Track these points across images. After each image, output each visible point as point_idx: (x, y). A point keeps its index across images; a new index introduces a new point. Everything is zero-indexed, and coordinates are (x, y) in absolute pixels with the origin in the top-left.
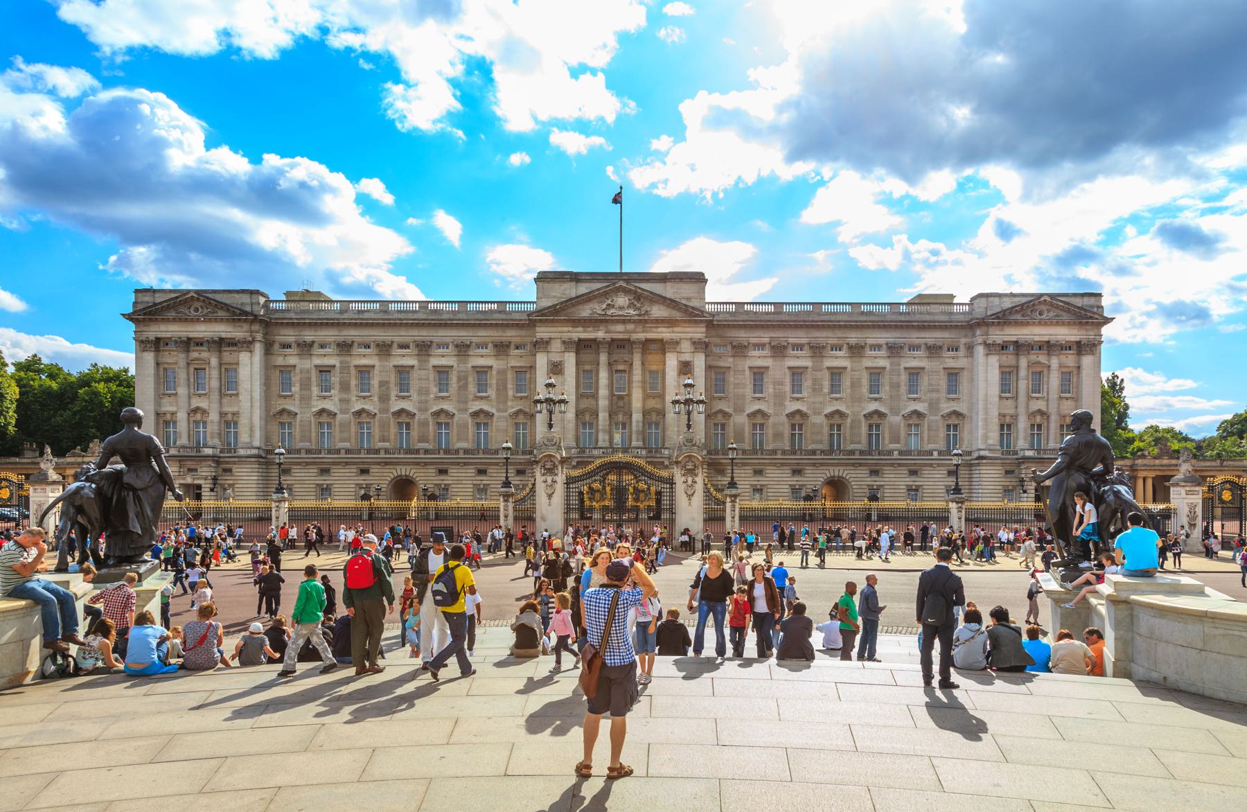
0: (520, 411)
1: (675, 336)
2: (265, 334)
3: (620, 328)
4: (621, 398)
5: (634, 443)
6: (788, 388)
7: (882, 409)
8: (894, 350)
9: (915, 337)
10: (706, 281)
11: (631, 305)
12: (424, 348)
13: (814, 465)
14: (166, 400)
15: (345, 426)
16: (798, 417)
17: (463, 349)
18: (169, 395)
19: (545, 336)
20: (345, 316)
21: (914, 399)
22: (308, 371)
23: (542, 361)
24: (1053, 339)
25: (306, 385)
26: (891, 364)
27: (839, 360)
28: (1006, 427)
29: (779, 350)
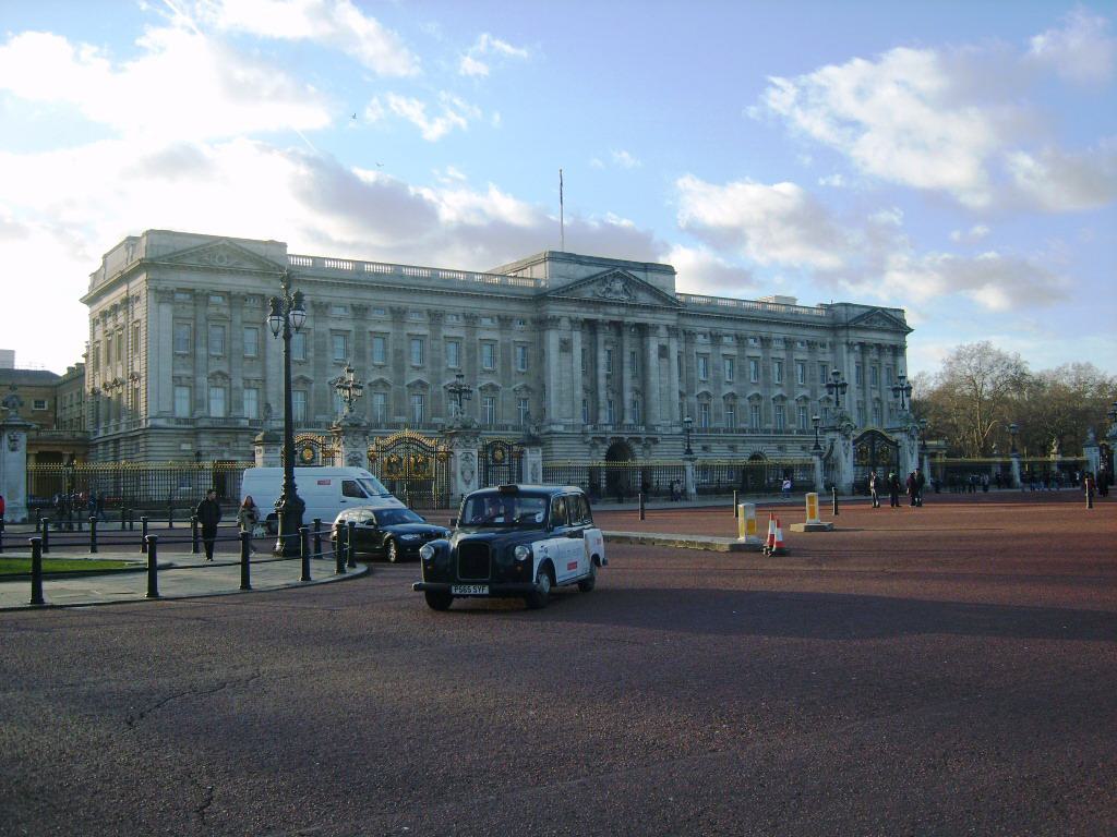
0: (525, 386)
3: (615, 310)
8: (789, 343)
10: (674, 273)
12: (436, 317)
13: (744, 442)
17: (471, 320)
18: (184, 356)
19: (557, 314)
20: (362, 278)
21: (802, 386)
22: (324, 335)
23: (553, 339)
25: (321, 351)
26: (788, 355)
27: (755, 351)
28: (861, 409)
29: (716, 339)
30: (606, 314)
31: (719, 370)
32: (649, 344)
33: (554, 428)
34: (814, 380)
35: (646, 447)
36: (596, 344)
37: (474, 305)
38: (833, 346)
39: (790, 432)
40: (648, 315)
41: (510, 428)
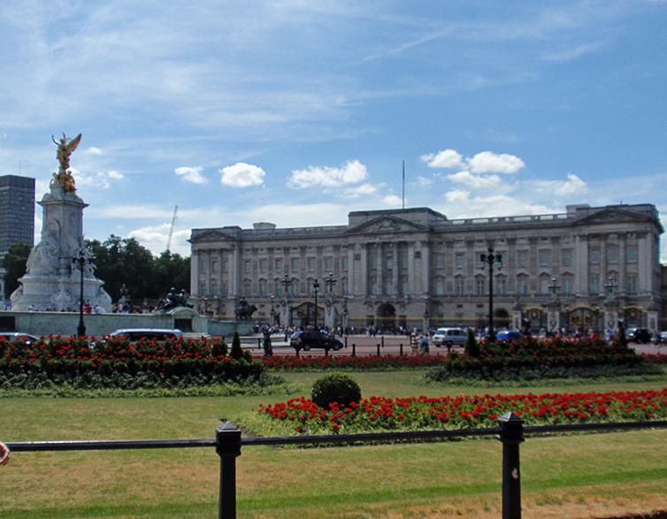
1: (412, 240)
2: (239, 246)
3: (386, 236)
4: (390, 270)
5: (394, 293)
6: (475, 262)
7: (527, 273)
8: (533, 240)
9: (545, 233)
11: (391, 226)
14: (202, 275)
15: (271, 285)
17: (320, 249)
24: (619, 231)
25: (255, 268)
26: (532, 248)
29: (470, 243)
30: (381, 239)
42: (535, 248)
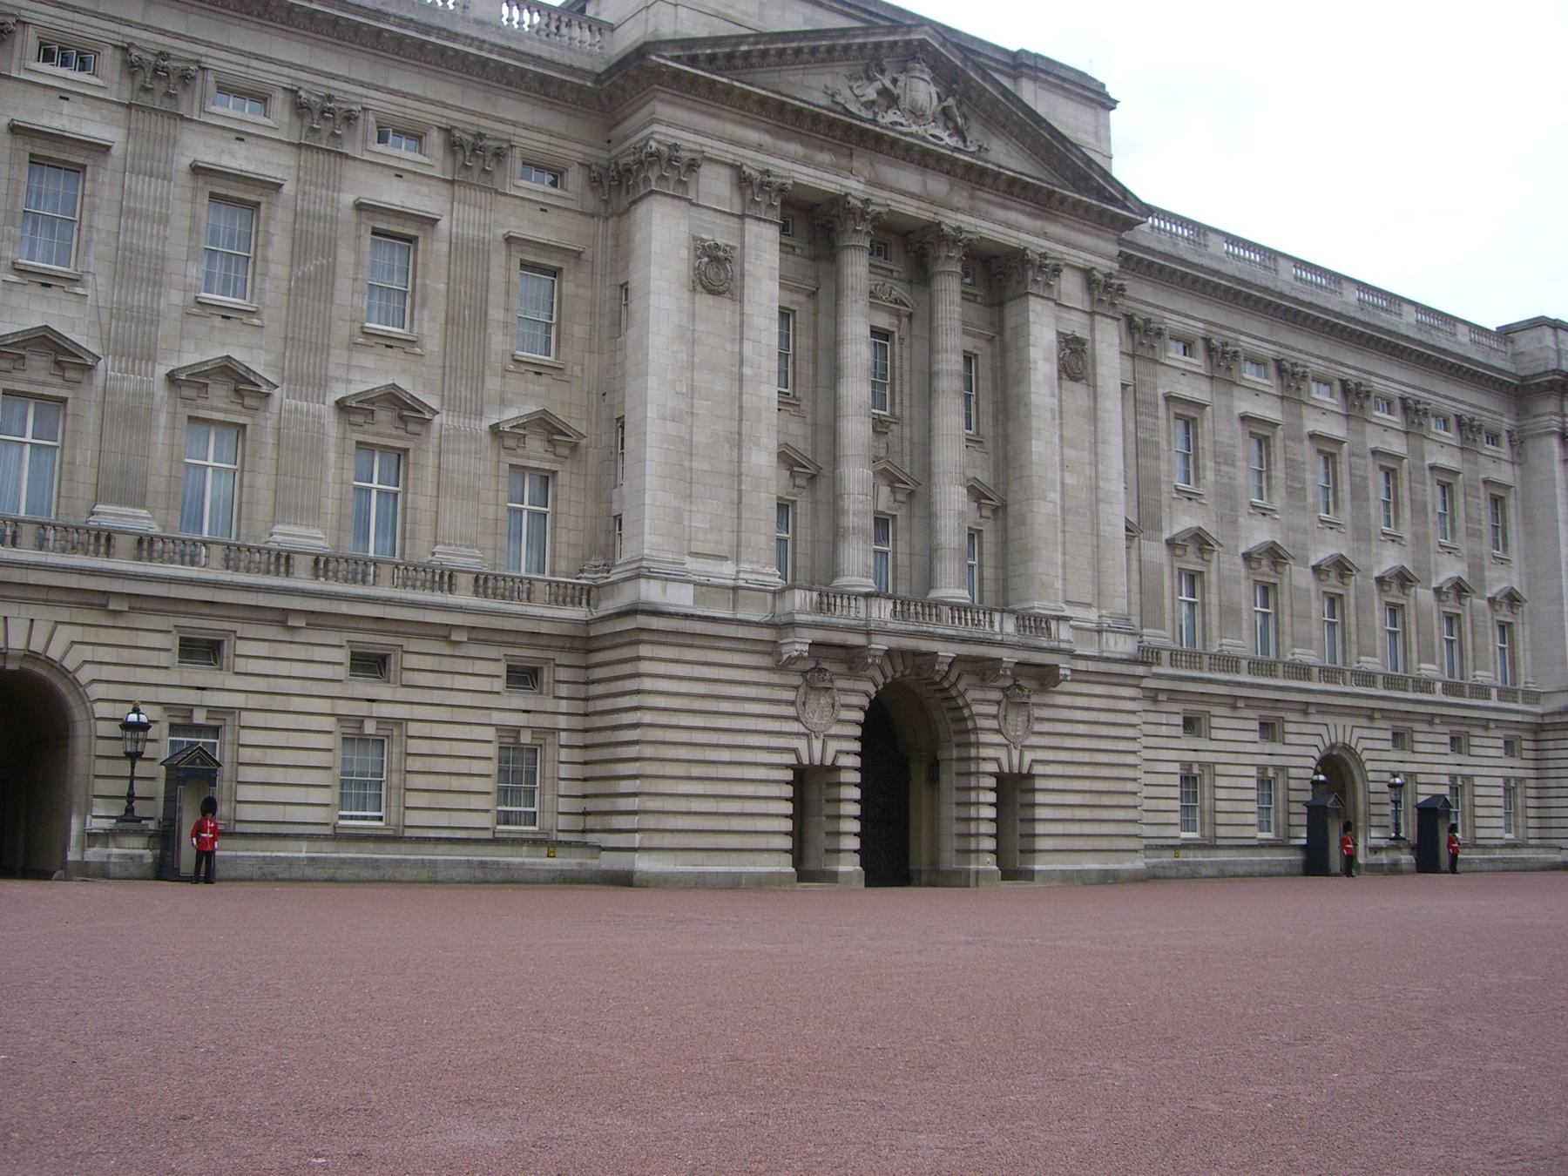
3: (908, 178)
6: (1243, 476)
16: (1265, 566)
19: (688, 140)
21: (1450, 550)
23: (664, 233)
27: (1324, 417)
29: (1221, 360)
31: (1233, 465)
32: (1023, 329)
33: (650, 592)
34: (1474, 534)
35: (1013, 699)
36: (837, 295)
37: (343, 72)
38: (1519, 442)
39: (1425, 685)
40: (1023, 220)
41: (464, 581)
42: (1422, 458)
